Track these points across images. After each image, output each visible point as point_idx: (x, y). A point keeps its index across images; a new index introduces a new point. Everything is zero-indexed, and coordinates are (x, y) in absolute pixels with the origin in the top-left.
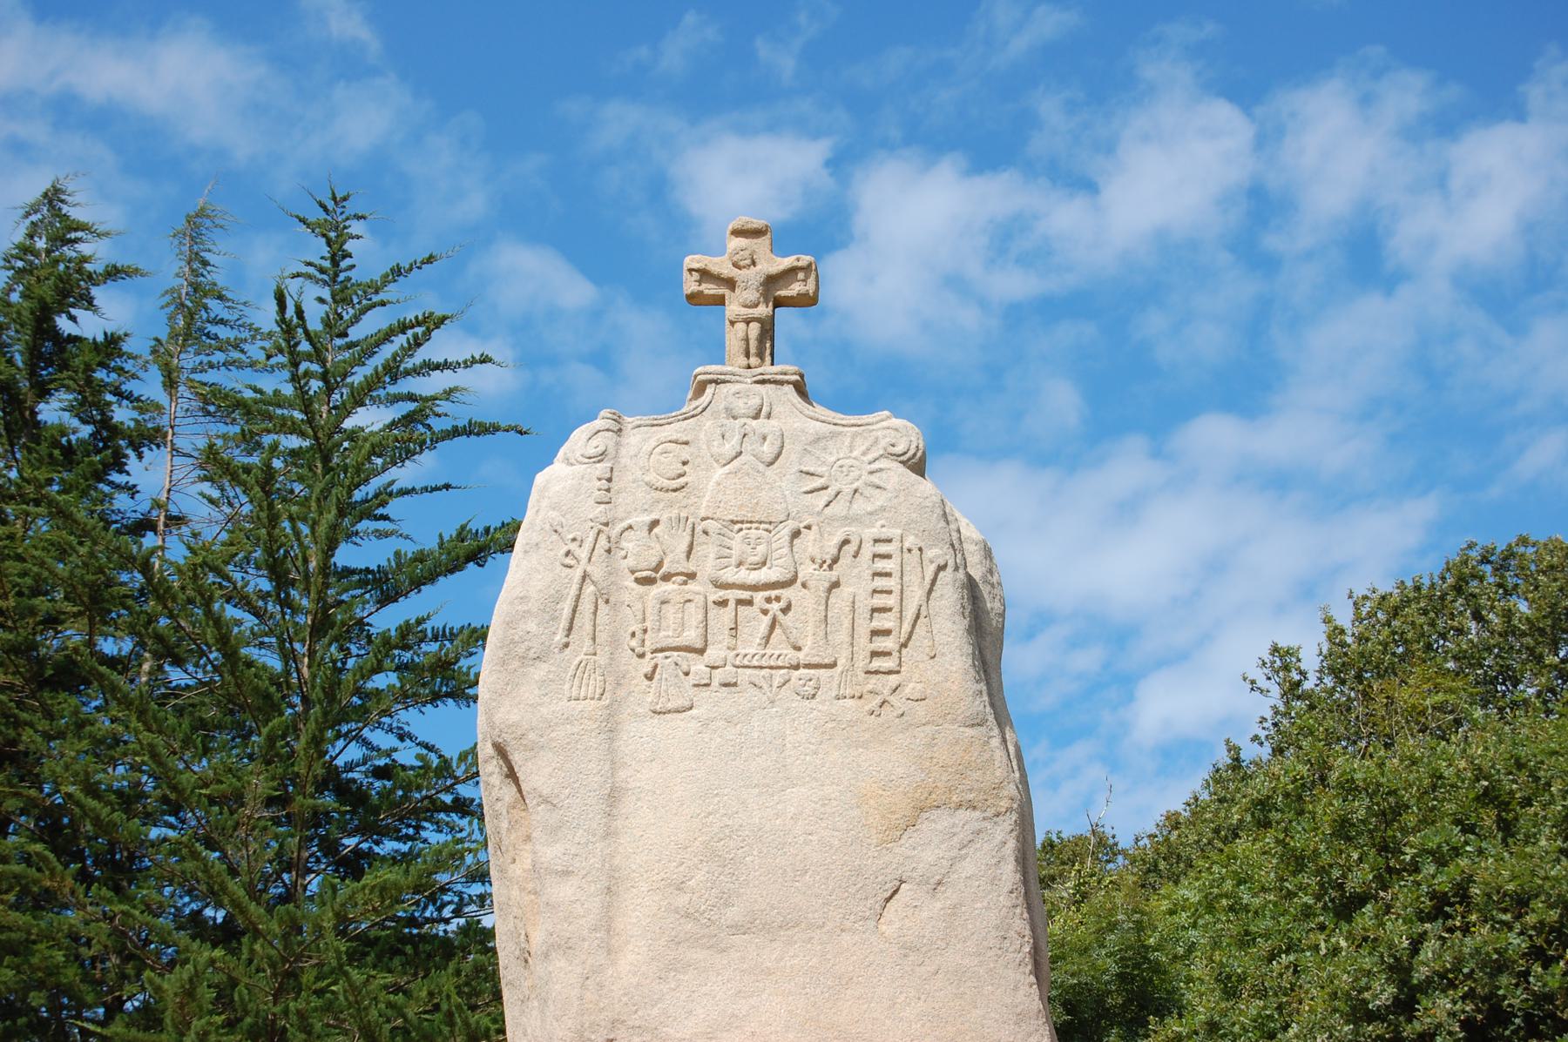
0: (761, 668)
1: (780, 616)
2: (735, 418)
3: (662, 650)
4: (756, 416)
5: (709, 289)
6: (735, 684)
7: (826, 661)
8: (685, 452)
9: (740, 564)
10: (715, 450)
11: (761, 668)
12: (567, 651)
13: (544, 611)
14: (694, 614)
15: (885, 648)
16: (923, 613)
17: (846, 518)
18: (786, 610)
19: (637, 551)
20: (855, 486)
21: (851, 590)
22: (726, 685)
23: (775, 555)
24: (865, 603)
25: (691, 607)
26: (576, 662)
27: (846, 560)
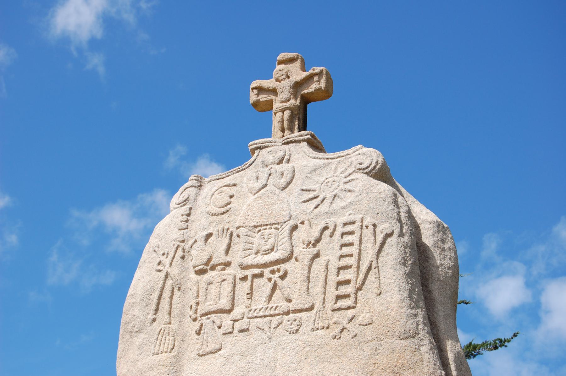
0: (265, 316)
1: (279, 281)
2: (267, 166)
3: (206, 314)
4: (280, 162)
5: (263, 98)
6: (247, 330)
7: (306, 306)
8: (233, 191)
9: (257, 253)
11: (265, 316)
12: (155, 324)
14: (227, 288)
15: (347, 291)
16: (374, 265)
18: (283, 277)
19: (198, 255)
20: (334, 193)
21: (327, 258)
22: (242, 331)
23: (280, 243)
24: (334, 265)
26: (159, 330)
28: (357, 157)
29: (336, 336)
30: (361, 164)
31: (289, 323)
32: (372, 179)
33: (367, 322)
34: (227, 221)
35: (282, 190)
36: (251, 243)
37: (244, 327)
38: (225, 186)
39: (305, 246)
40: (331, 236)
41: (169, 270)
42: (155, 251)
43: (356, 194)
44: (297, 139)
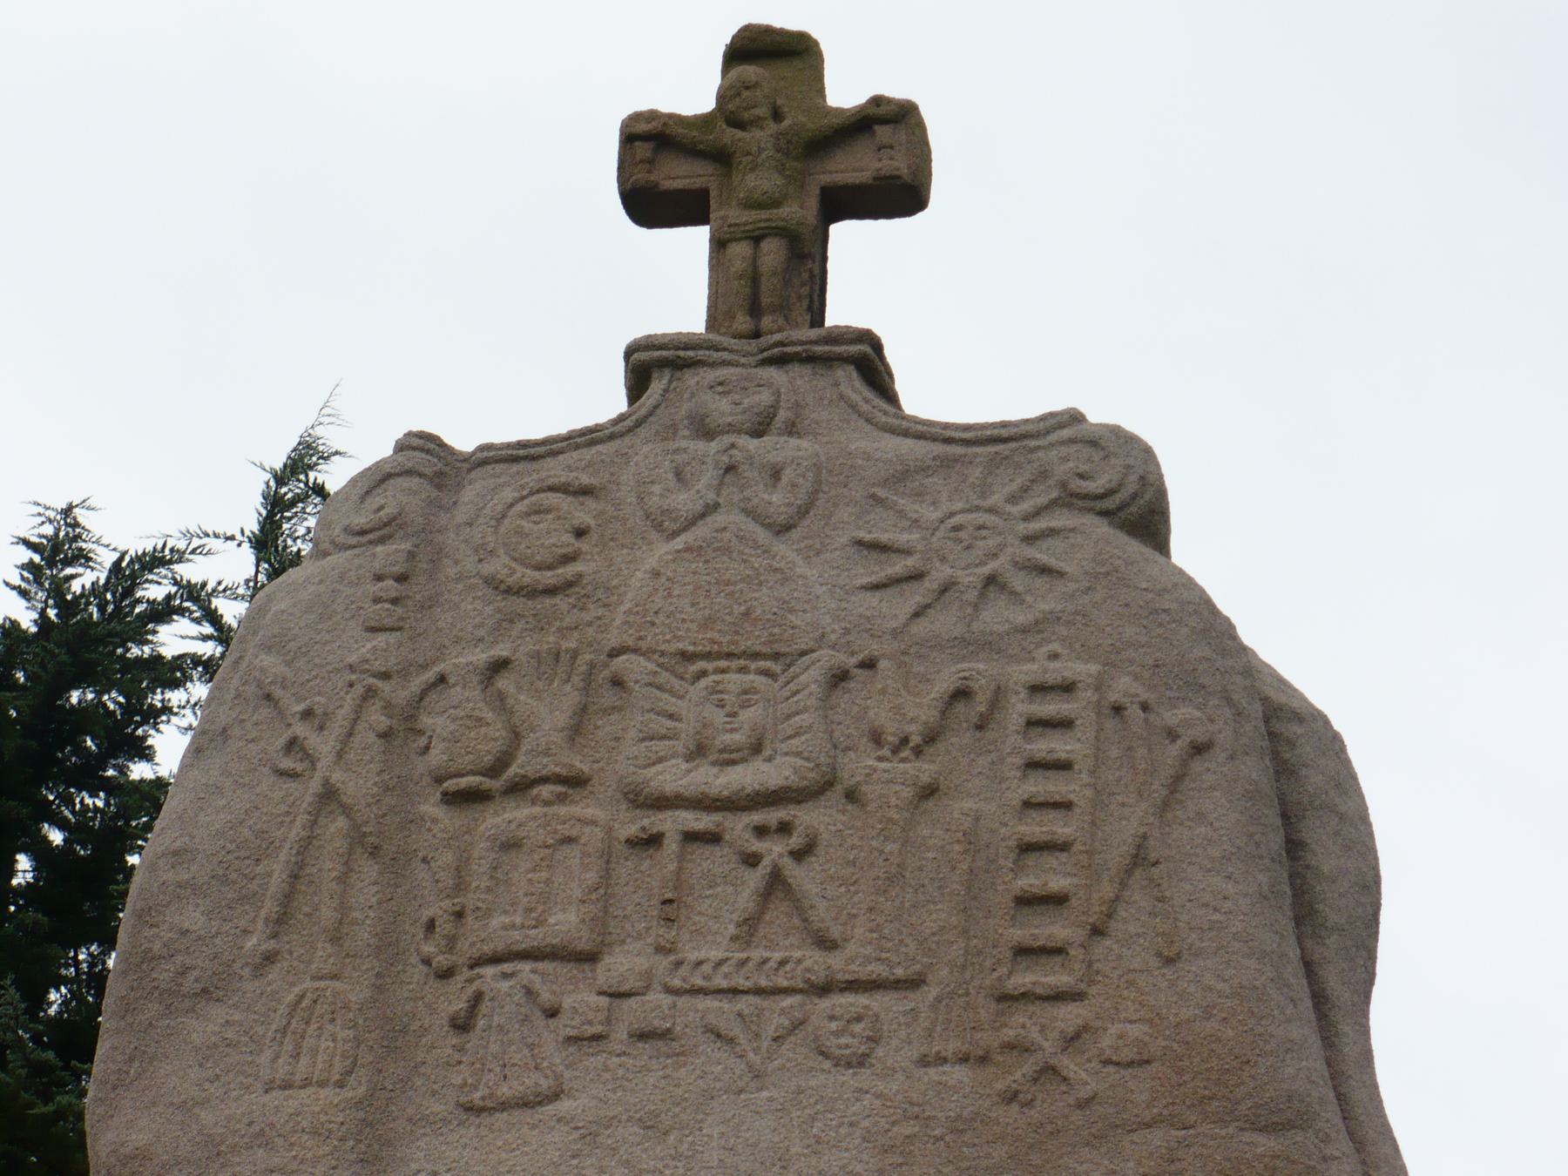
0: (735, 992)
3: (495, 960)
7: (899, 972)
8: (583, 514)
10: (654, 502)
11: (735, 992)
12: (274, 973)
13: (224, 880)
17: (963, 642)
20: (986, 570)
22: (643, 1036)
25: (572, 854)
26: (291, 998)
27: (959, 740)
28: (1064, 450)
29: (1016, 1094)
30: (1081, 476)
31: (834, 1026)
32: (1123, 538)
33: (1127, 1054)
34: (567, 621)
35: (778, 533)
36: (671, 717)
37: (656, 1023)
38: (551, 489)
39: (886, 752)
40: (980, 727)
41: (337, 777)
42: (268, 697)
43: (1072, 586)
44: (819, 349)
